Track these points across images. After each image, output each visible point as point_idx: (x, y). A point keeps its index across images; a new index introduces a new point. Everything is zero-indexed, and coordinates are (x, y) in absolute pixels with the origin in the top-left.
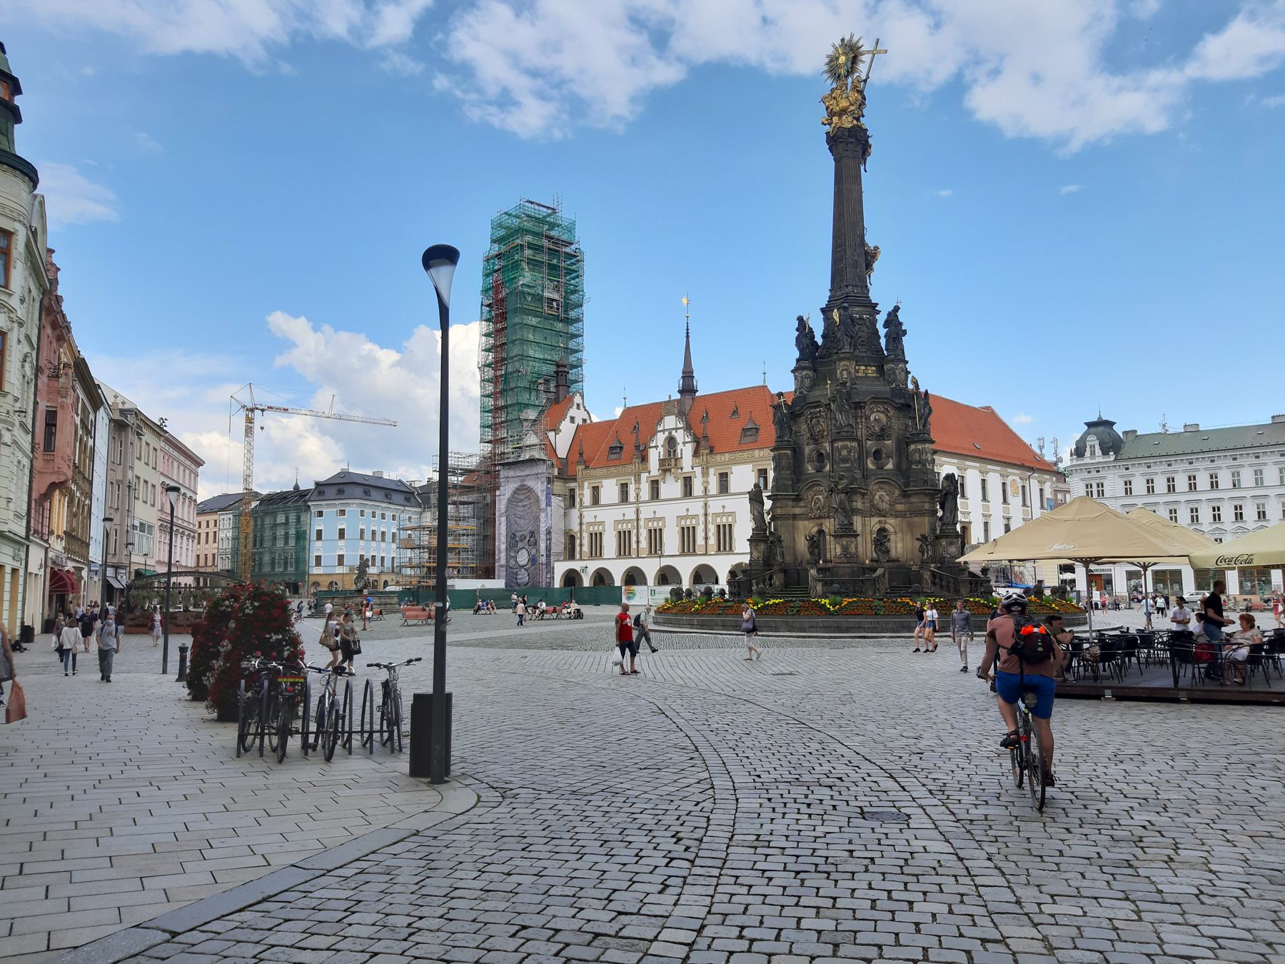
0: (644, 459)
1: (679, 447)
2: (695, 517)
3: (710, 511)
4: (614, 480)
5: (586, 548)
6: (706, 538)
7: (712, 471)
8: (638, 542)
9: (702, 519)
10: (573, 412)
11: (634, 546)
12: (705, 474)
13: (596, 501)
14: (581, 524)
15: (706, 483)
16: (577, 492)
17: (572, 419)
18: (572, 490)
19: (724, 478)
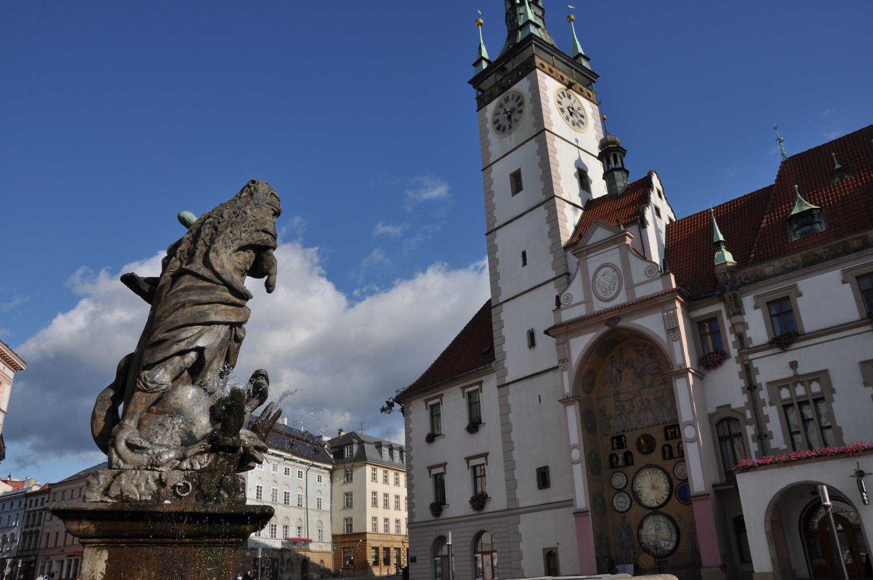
4: (833, 276)
5: (778, 441)
13: (787, 334)
14: (751, 388)
16: (727, 324)
18: (713, 320)
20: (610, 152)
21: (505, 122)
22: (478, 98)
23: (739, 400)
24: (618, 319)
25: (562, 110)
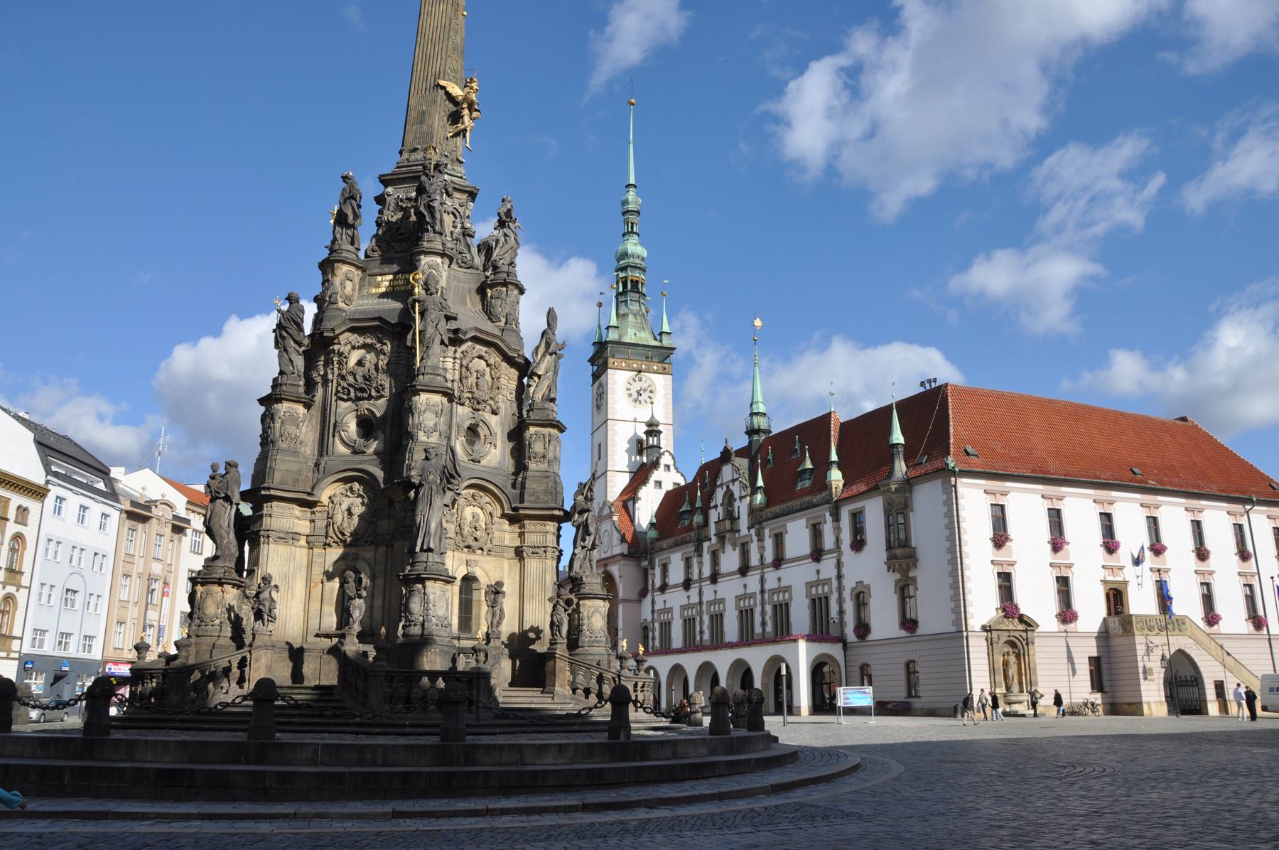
0: (706, 523)
1: (737, 504)
2: (752, 595)
3: (768, 586)
6: (764, 624)
7: (767, 532)
8: (701, 632)
9: (759, 597)
10: (656, 475)
11: (698, 638)
12: (761, 539)
14: (653, 611)
15: (762, 548)
16: (650, 572)
17: (659, 484)
19: (779, 539)
20: (653, 429)
23: (649, 619)
24: (605, 565)
25: (630, 395)
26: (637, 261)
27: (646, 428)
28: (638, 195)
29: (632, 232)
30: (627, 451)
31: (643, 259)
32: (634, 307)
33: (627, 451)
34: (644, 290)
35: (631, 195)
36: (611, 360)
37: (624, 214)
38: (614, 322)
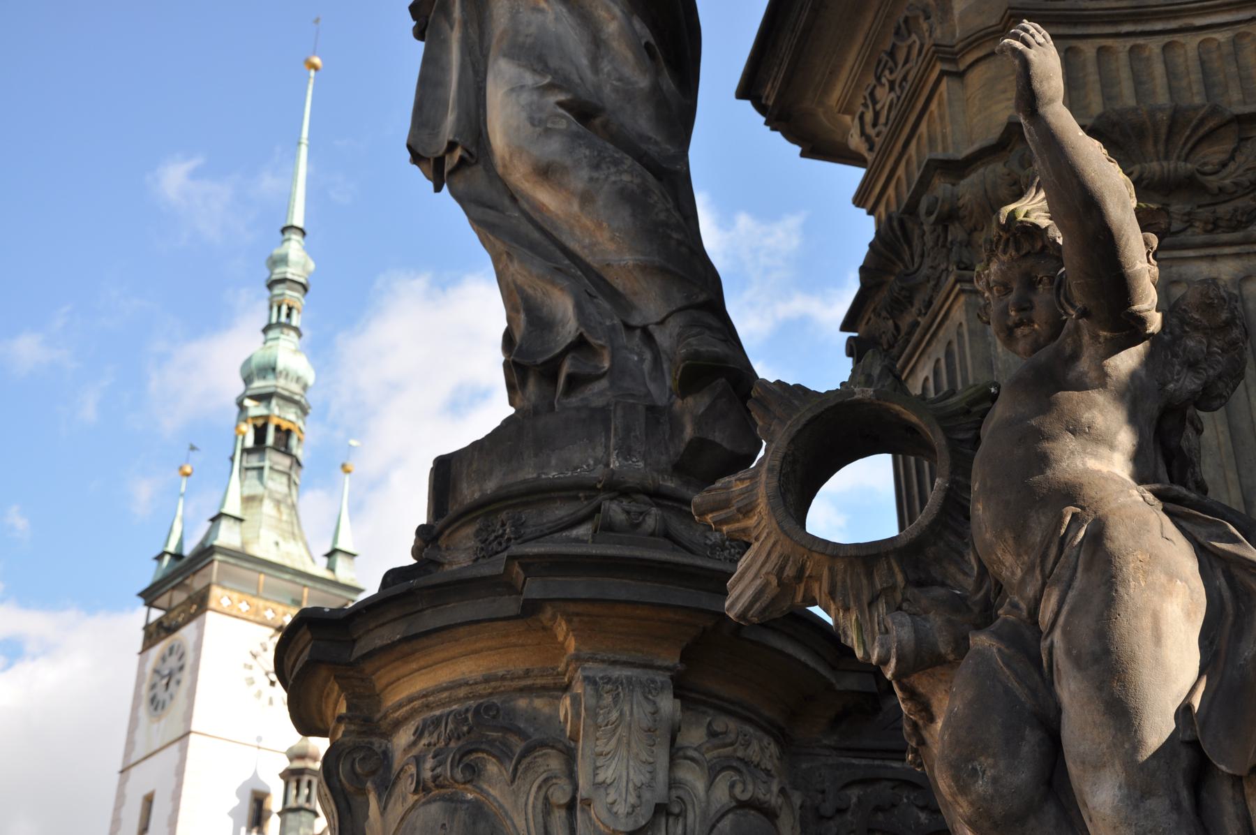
21: (162, 695)
22: (147, 628)
25: (251, 682)
26: (295, 388)
27: (285, 764)
28: (307, 249)
29: (288, 326)
30: (233, 813)
31: (305, 387)
32: (277, 484)
33: (233, 813)
34: (298, 451)
35: (294, 248)
36: (216, 592)
37: (271, 285)
38: (233, 506)
